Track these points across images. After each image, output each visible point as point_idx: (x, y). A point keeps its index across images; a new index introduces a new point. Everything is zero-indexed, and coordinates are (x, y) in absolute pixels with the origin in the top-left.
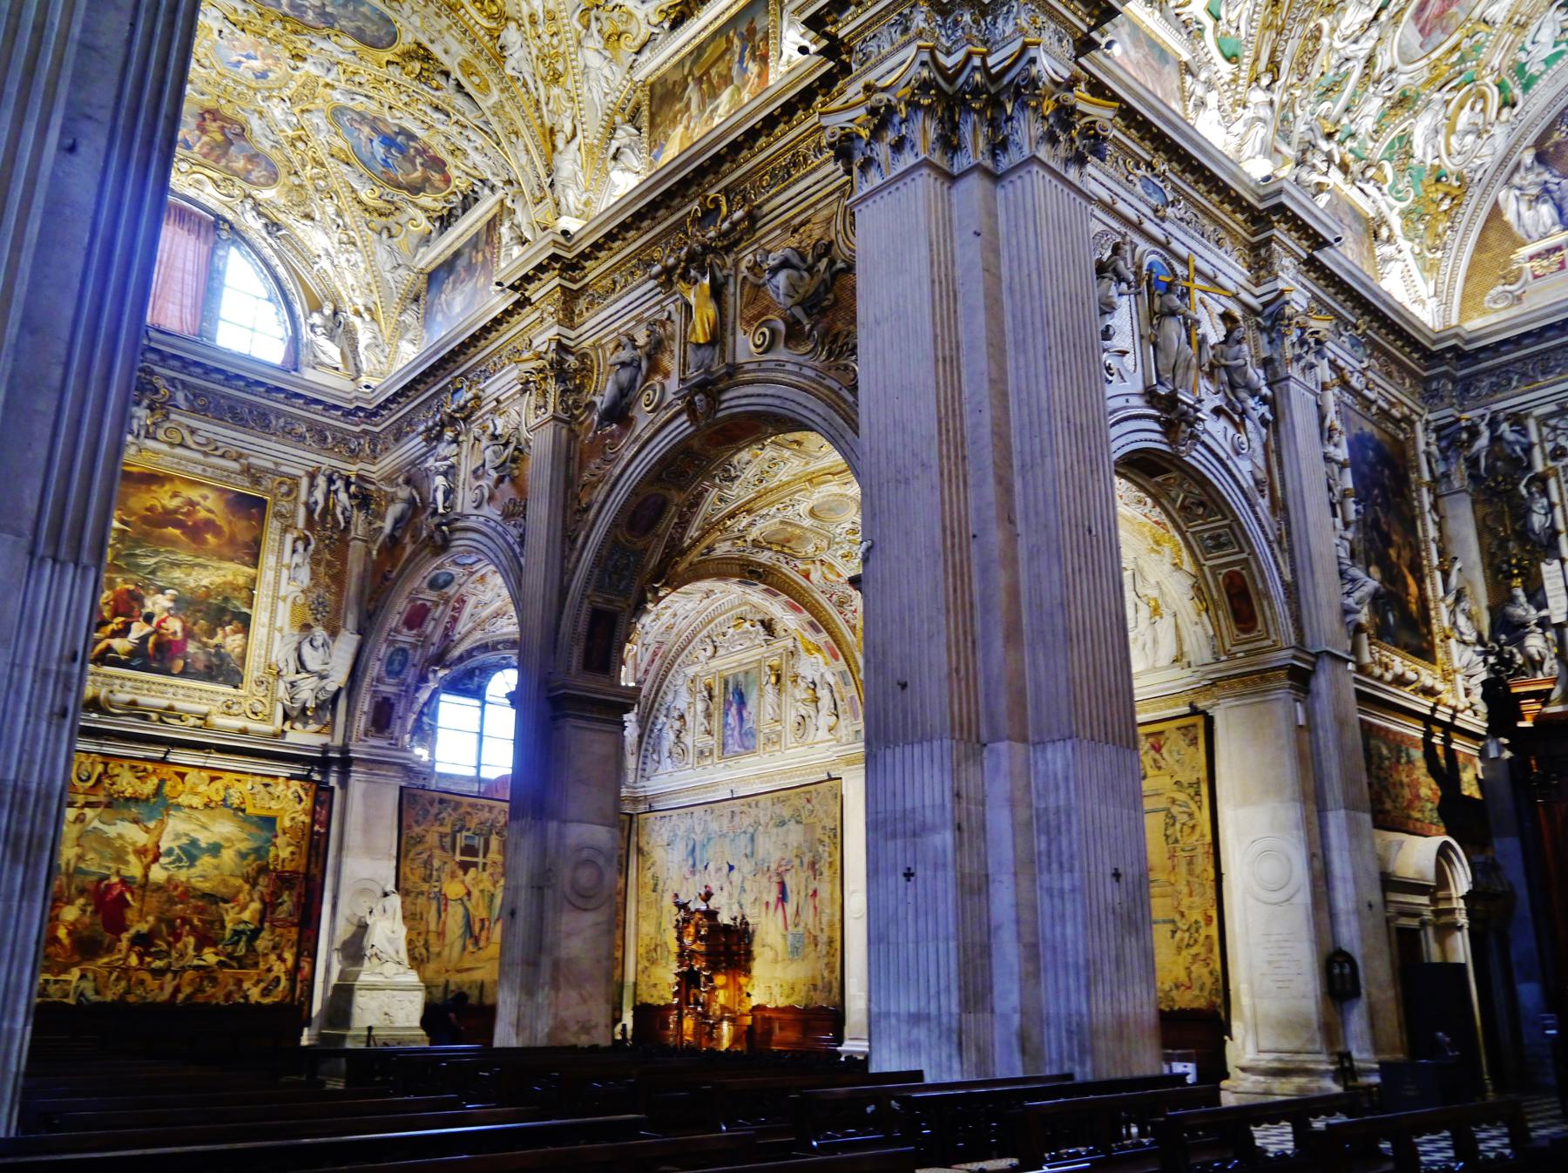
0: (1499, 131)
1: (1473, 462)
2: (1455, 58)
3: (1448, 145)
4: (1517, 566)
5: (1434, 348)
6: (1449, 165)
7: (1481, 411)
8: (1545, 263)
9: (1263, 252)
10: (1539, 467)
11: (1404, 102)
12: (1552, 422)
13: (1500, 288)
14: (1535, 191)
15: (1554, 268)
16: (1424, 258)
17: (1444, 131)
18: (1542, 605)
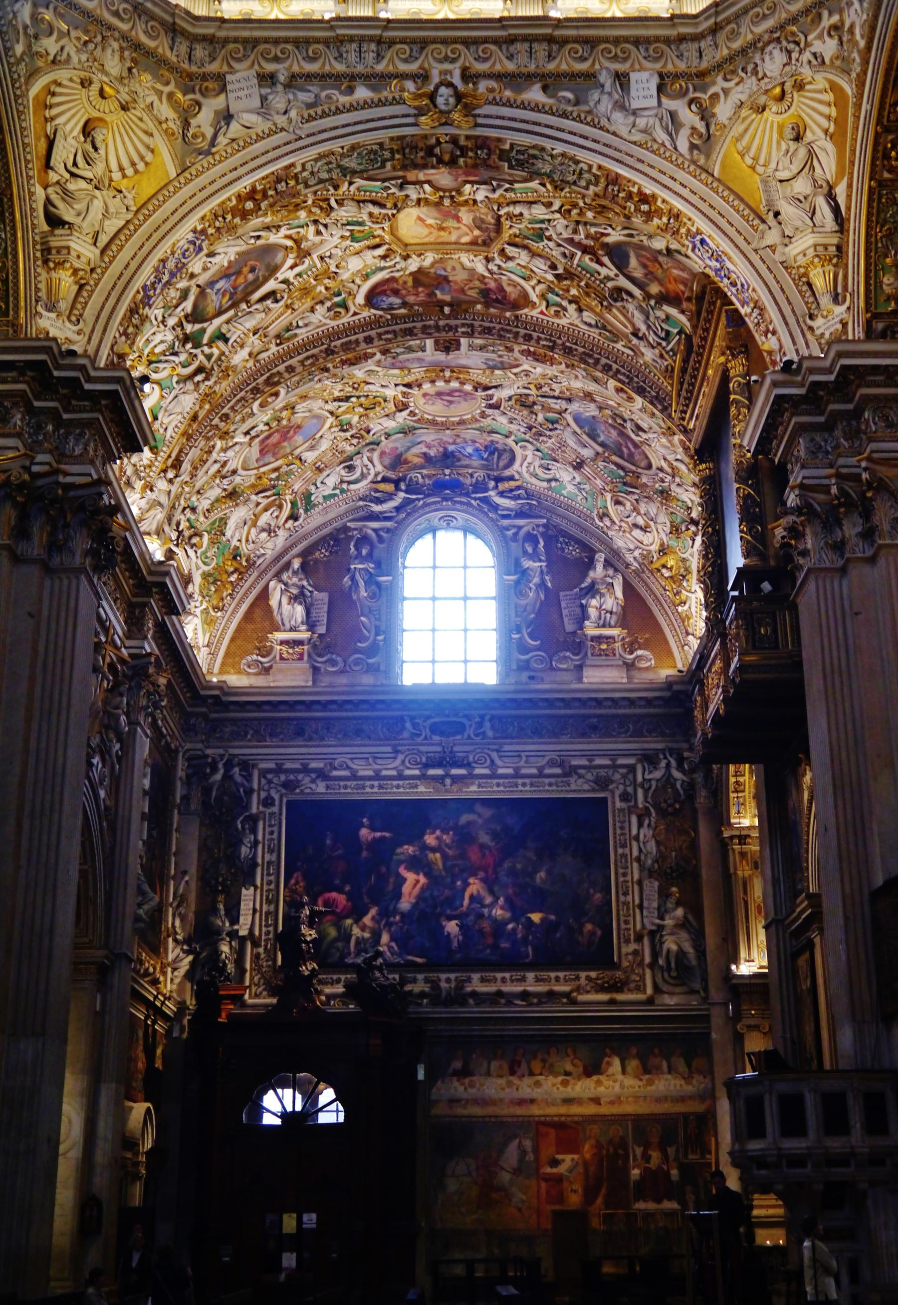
0: (282, 534)
1: (207, 791)
2: (274, 475)
3: (249, 533)
4: (222, 884)
5: (202, 693)
6: (245, 549)
7: (221, 751)
8: (291, 651)
9: (137, 612)
10: (254, 810)
11: (233, 495)
12: (269, 776)
13: (255, 657)
14: (295, 591)
15: (295, 657)
16: (208, 613)
17: (249, 523)
18: (235, 920)
